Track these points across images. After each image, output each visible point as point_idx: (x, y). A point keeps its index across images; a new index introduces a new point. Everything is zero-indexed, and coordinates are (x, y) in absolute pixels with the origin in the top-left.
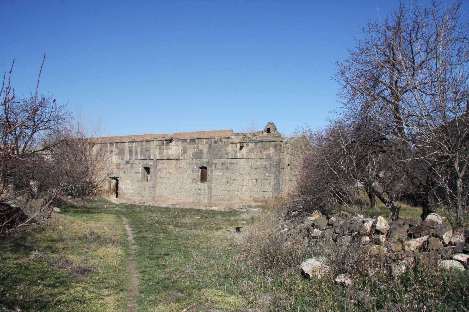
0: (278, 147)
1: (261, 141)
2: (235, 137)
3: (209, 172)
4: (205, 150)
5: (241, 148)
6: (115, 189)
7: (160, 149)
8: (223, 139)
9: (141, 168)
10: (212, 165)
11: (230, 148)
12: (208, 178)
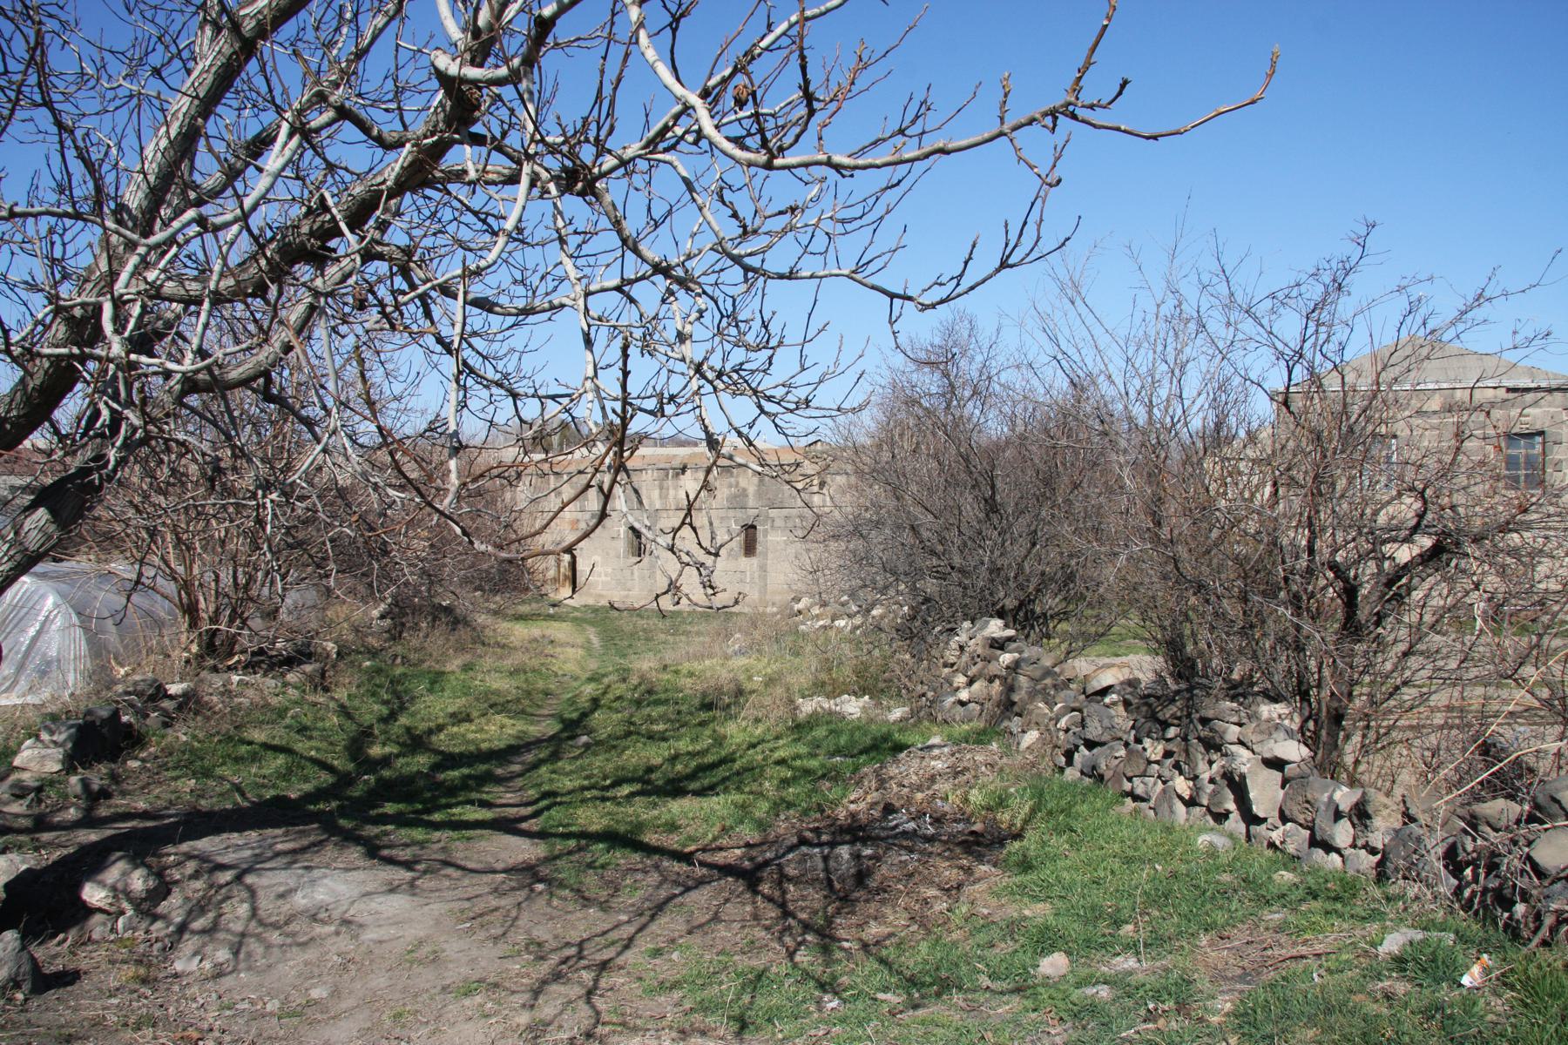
3: (760, 537)
4: (751, 490)
6: (569, 574)
7: (661, 488)
9: (623, 529)
10: (765, 522)
12: (759, 548)
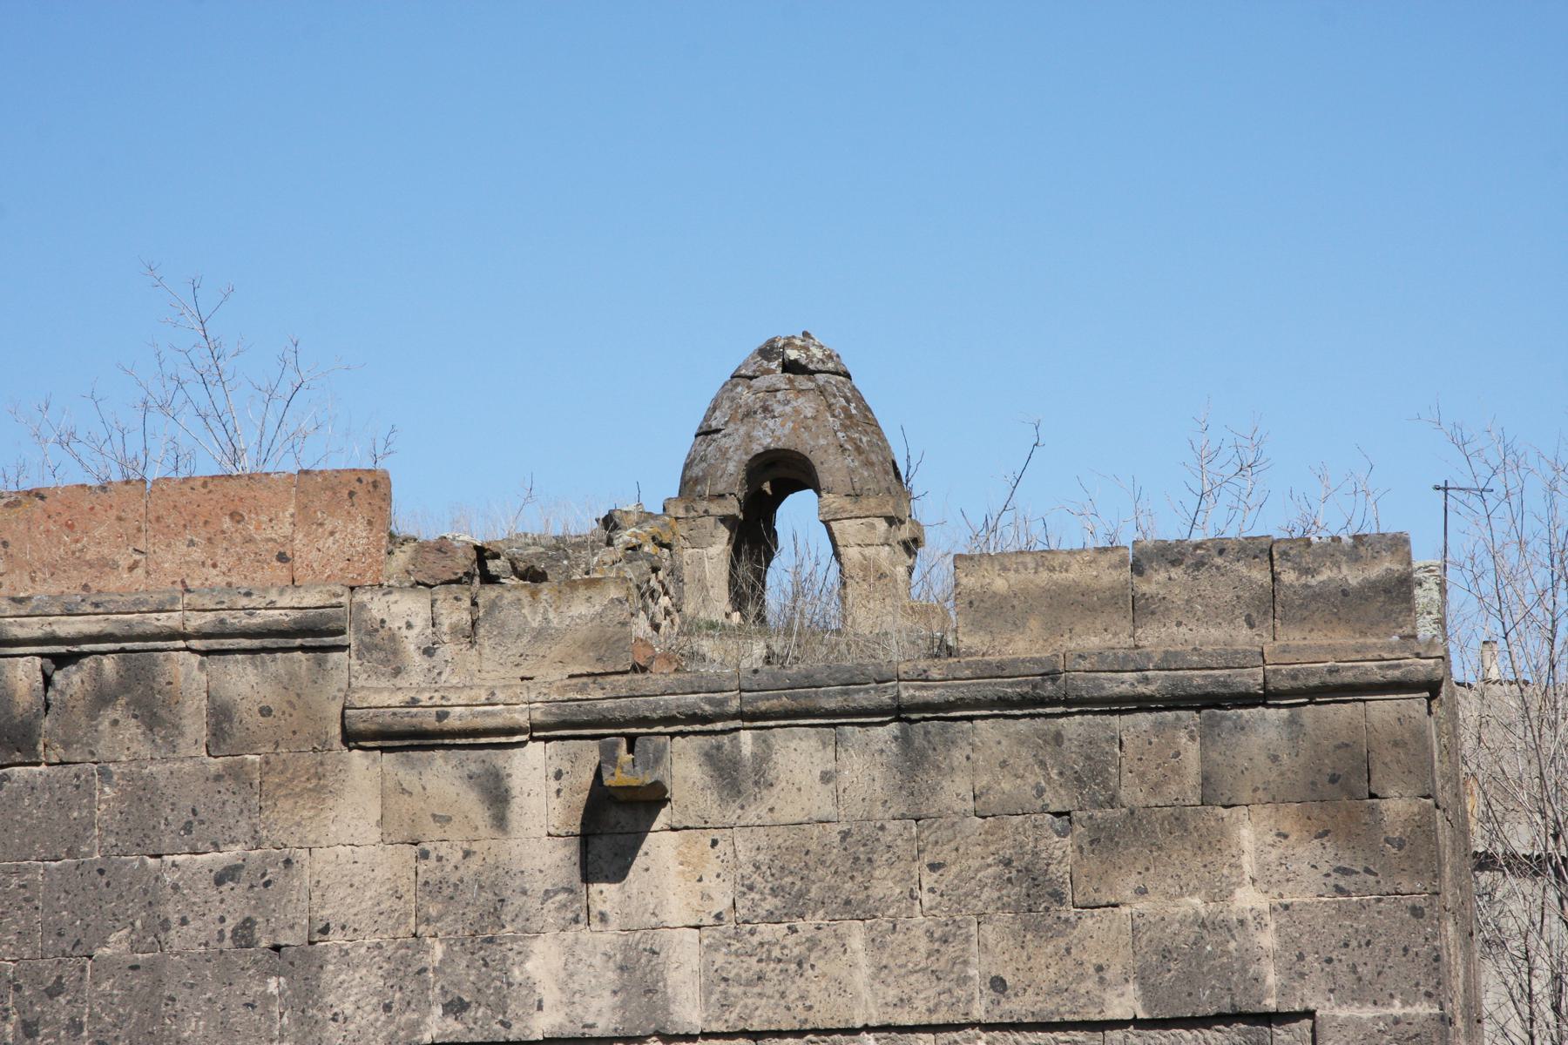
0: (1397, 806)
1: (1036, 698)
2: (455, 613)
5: (612, 827)
8: (184, 670)
11: (352, 841)
